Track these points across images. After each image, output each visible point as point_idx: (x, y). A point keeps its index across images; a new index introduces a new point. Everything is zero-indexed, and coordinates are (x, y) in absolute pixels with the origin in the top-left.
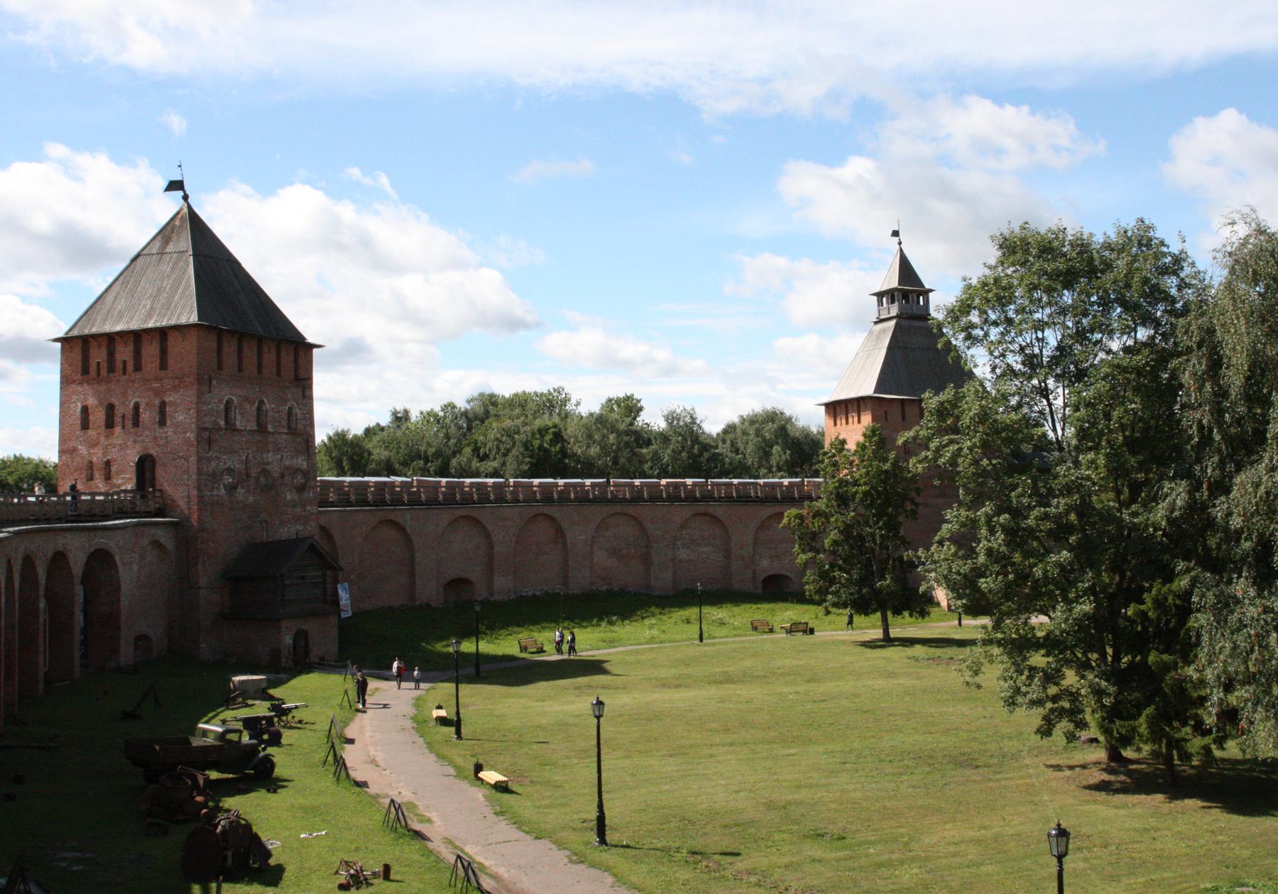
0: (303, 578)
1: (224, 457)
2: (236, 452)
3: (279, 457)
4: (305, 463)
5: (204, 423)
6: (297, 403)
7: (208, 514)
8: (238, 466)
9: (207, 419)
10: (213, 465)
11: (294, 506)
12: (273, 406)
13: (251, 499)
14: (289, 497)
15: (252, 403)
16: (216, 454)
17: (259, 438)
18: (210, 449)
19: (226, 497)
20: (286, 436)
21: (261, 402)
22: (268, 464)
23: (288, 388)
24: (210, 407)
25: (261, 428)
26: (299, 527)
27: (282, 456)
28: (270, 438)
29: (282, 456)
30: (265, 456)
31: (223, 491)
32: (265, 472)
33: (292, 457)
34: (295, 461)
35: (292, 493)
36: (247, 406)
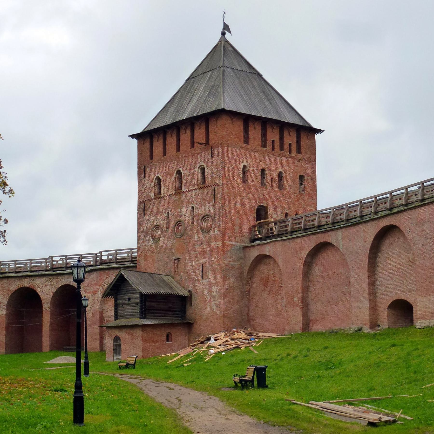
0: (129, 299)
1: (153, 218)
2: (160, 212)
3: (190, 208)
4: (212, 209)
5: (141, 199)
6: (206, 163)
7: (143, 258)
8: (163, 223)
9: (144, 195)
10: (147, 224)
11: (201, 244)
12: (187, 172)
13: (169, 243)
14: (196, 238)
15: (171, 175)
16: (149, 217)
17: (176, 199)
18: (144, 215)
19: (153, 245)
20: (196, 191)
21: (179, 172)
22: (182, 216)
23: (199, 154)
24: (145, 187)
25: (179, 190)
26: (204, 260)
27: (193, 207)
28: (184, 196)
29: (193, 207)
30: (180, 210)
31: (152, 241)
32: (179, 224)
33: (200, 206)
34: (202, 209)
35: (199, 233)
36: (168, 178)
